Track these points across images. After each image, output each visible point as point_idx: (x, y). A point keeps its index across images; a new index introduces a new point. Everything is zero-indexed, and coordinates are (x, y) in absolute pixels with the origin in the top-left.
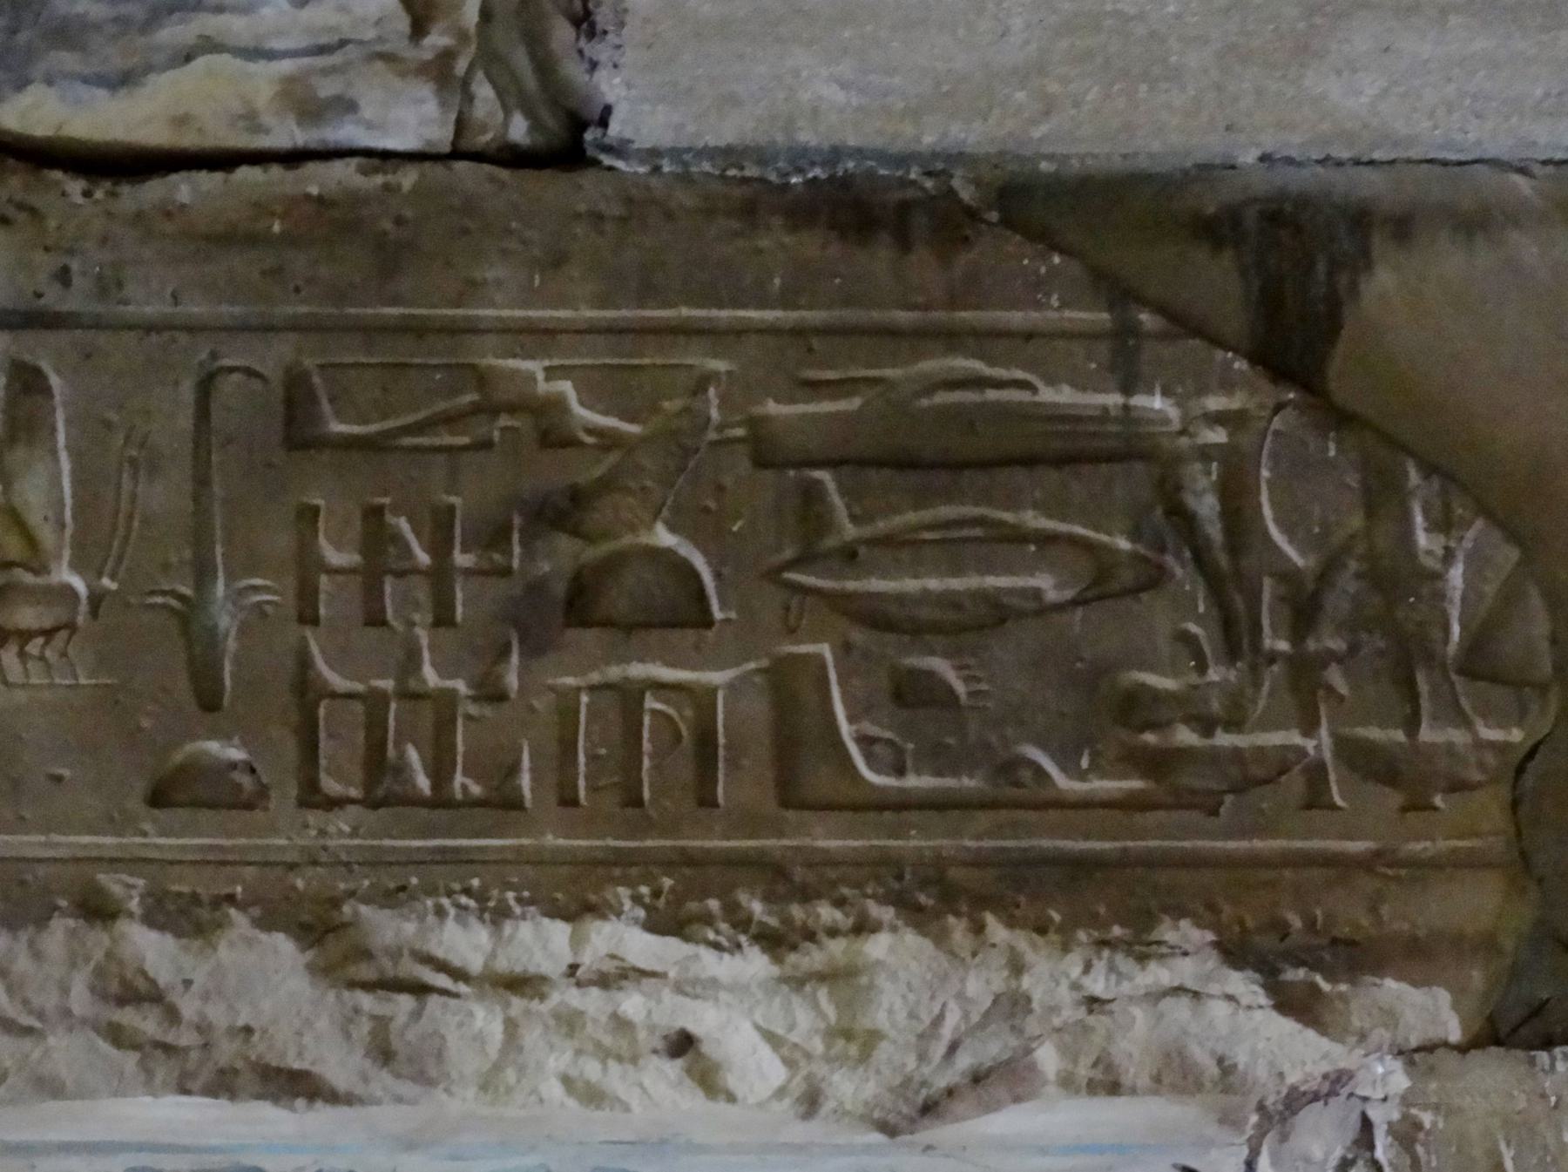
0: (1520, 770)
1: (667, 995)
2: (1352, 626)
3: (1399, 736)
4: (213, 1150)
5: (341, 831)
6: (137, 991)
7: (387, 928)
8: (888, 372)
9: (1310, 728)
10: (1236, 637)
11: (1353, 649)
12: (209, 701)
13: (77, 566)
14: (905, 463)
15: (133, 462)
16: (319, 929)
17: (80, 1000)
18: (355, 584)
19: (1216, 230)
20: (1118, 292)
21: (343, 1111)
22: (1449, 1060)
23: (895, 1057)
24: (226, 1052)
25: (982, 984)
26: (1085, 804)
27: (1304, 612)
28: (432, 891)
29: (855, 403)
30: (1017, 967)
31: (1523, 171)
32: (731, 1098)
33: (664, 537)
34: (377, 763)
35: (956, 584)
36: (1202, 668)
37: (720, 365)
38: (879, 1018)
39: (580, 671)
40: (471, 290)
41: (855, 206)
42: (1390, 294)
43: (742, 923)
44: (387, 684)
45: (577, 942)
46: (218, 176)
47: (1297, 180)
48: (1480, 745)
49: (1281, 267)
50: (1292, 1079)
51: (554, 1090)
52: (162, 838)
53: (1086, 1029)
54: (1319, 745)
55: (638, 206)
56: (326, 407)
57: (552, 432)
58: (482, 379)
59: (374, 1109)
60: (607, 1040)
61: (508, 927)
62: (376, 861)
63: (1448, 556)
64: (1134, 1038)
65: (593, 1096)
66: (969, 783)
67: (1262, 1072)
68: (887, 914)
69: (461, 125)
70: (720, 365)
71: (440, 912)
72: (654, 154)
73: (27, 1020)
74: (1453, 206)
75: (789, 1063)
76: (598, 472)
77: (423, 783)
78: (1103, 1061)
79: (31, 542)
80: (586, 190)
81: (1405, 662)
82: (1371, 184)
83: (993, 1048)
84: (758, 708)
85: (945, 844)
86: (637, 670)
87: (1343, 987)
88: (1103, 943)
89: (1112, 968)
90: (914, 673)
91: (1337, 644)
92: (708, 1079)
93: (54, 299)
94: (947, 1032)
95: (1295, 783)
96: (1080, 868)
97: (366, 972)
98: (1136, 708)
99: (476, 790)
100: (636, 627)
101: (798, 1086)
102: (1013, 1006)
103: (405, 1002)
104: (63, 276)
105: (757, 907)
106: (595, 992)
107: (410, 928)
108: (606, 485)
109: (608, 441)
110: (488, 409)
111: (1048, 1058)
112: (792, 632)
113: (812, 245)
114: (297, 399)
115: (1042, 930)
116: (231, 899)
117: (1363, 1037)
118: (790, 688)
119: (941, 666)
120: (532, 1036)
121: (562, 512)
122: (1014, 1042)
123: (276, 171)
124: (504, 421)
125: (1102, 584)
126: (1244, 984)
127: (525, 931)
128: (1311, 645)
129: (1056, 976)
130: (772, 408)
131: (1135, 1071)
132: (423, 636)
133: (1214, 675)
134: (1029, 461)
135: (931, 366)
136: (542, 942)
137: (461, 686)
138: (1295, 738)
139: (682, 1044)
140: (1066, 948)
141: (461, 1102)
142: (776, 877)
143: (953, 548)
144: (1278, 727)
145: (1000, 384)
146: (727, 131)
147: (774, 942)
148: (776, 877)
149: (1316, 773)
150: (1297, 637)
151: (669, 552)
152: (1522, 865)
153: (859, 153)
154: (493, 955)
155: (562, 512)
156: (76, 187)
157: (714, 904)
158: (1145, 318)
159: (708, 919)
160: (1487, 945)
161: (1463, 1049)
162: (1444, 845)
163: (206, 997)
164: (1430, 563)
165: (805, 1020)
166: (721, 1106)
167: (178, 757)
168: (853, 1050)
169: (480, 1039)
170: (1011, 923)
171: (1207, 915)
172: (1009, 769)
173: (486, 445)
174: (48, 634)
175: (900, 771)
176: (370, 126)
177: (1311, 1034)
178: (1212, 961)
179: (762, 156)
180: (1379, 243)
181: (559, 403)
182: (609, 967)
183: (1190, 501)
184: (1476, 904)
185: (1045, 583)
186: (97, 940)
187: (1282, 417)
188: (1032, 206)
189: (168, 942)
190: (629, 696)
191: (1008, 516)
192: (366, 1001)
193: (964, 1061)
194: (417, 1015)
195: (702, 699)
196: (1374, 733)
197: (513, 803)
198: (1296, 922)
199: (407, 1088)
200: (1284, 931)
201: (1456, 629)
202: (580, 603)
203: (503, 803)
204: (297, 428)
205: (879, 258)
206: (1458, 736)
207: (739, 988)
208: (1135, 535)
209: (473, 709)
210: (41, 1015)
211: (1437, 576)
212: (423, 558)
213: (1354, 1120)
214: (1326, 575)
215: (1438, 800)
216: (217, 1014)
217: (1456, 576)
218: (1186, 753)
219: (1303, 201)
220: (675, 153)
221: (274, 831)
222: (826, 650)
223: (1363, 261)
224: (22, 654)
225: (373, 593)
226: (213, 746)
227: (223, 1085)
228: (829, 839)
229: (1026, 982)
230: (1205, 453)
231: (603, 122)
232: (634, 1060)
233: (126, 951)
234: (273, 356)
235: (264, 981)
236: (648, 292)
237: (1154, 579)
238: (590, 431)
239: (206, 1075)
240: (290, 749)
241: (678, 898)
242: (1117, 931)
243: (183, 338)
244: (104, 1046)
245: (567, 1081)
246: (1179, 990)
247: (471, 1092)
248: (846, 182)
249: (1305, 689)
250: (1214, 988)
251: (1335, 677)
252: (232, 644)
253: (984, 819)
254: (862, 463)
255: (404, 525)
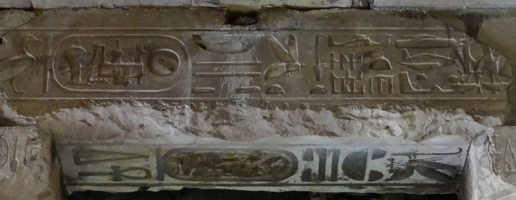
0: (508, 88)
1: (385, 120)
2: (483, 69)
3: (490, 84)
4: (320, 145)
5: (338, 97)
6: (309, 120)
7: (345, 110)
8: (415, 36)
9: (477, 83)
10: (466, 70)
11: (483, 72)
12: (318, 79)
13: (299, 62)
14: (417, 48)
15: (307, 48)
16: (335, 110)
17: (300, 121)
18: (339, 65)
19: (461, 17)
20: (446, 25)
21: (338, 138)
22: (500, 128)
23: (418, 129)
24: (321, 128)
25: (431, 118)
26: (445, 93)
27: (476, 68)
28: (351, 105)
29: (409, 40)
30: (436, 115)
31: (504, 9)
32: (394, 136)
33: (383, 58)
34: (343, 89)
35: (425, 64)
36: (461, 75)
37: (391, 35)
38: (416, 124)
39: (372, 75)
40: (355, 25)
41: (409, 14)
42: (485, 25)
43: (396, 109)
44: (344, 77)
45: (372, 112)
46: (318, 11)
47: (472, 11)
48: (502, 84)
49: (471, 23)
50: (476, 132)
51: (369, 134)
52: (312, 98)
53: (446, 125)
54: (479, 85)
55: (378, 14)
56: (334, 41)
57: (366, 43)
58: (356, 37)
59: (343, 138)
60: (376, 127)
61: (362, 110)
62: (344, 101)
63: (496, 60)
64: (453, 126)
65: (374, 135)
66: (429, 90)
67: (472, 131)
68: (417, 108)
69: (352, 3)
70: (391, 35)
71: (352, 108)
72: (380, 8)
73: (292, 124)
74: (495, 14)
75: (403, 130)
76: (373, 50)
77: (350, 91)
78: (449, 129)
79: (293, 59)
80: (370, 12)
81: (491, 73)
82: (483, 12)
83: (432, 128)
84: (397, 81)
85: (425, 99)
86: (380, 75)
87: (484, 118)
88: (448, 112)
89: (450, 116)
90: (420, 76)
91: (481, 71)
92: (391, 132)
93: (295, 27)
94: (426, 125)
95: (475, 90)
96: (444, 101)
97: (342, 116)
98: (452, 80)
99: (357, 91)
100: (379, 70)
101: (404, 134)
102: (435, 121)
103: (347, 121)
104: (296, 24)
105: (398, 107)
106: (375, 119)
107: (348, 110)
108: (375, 51)
109: (375, 45)
110: (358, 41)
111: (440, 129)
112: (402, 70)
113: (403, 19)
114: (330, 39)
115: (439, 110)
116: (322, 106)
117: (487, 125)
118: (402, 77)
119: (423, 74)
120: (366, 126)
121: (369, 54)
122: (436, 127)
123: (326, 10)
124: (360, 42)
125: (446, 63)
126: (469, 118)
127: (365, 110)
128: (477, 72)
129: (442, 117)
130: (398, 41)
131: (453, 132)
132: (349, 71)
133: (463, 76)
134: (435, 47)
135: (420, 35)
136: (367, 112)
137: (354, 77)
138: (475, 84)
139: (387, 128)
140: (443, 112)
141: (355, 136)
142: (401, 103)
143: (424, 59)
144: (473, 82)
145: (430, 37)
146: (390, 4)
147: (401, 112)
148: (401, 103)
149: (479, 88)
150: (475, 71)
151: (384, 60)
152: (509, 102)
153: (409, 7)
154: (360, 114)
155: (369, 54)
156: (298, 12)
157: (392, 106)
158: (451, 28)
159: (391, 109)
160: (504, 112)
161: (502, 126)
162: (497, 98)
163: (318, 120)
164: (494, 61)
165: (405, 123)
166: (393, 137)
167: (314, 87)
168: (412, 128)
169: (358, 127)
170: (435, 109)
171: (463, 108)
172: (434, 88)
173: (357, 45)
174: (295, 71)
175: (418, 89)
176: (340, 3)
177: (479, 124)
178: (465, 114)
179: (396, 8)
180: (484, 19)
181: (368, 40)
182: (377, 116)
183: (459, 53)
184: (503, 106)
185: (438, 64)
186: (303, 112)
187: (472, 41)
188: (434, 14)
189: (313, 112)
190: (379, 79)
191: (432, 55)
192: (342, 121)
193: (428, 130)
194: (349, 123)
195: (389, 80)
196: (486, 83)
197: (363, 93)
198: (477, 109)
199: (348, 134)
200: (475, 110)
201: (498, 69)
202: (371, 66)
203: (361, 93)
204: (330, 43)
205: (413, 20)
206: (498, 84)
207: (396, 119)
208: (451, 57)
209: (356, 81)
210: (295, 123)
211: (494, 64)
212: (349, 60)
213: (486, 137)
214: (478, 62)
215: (496, 92)
216: (320, 123)
217: (497, 62)
218: (460, 86)
219: (473, 13)
220: (383, 7)
221: (328, 97)
222: (407, 72)
223: (482, 21)
224: (291, 74)
225: (342, 65)
226: (319, 86)
227: (321, 134)
228: (408, 98)
229: (437, 118)
230: (460, 46)
231: (373, 3)
232: (380, 130)
233: (307, 114)
234: (326, 35)
235: (327, 118)
236: (379, 25)
237: (454, 63)
238: (372, 44)
239: (318, 132)
240: (330, 85)
241: (387, 106)
242: (450, 110)
243: (314, 32)
244: (304, 128)
245: (371, 133)
246: (459, 119)
247: (357, 135)
248: (407, 11)
249: (476, 77)
250: (465, 118)
251: (480, 76)
252: (321, 72)
253: (431, 95)
254: (412, 48)
255: (346, 56)
